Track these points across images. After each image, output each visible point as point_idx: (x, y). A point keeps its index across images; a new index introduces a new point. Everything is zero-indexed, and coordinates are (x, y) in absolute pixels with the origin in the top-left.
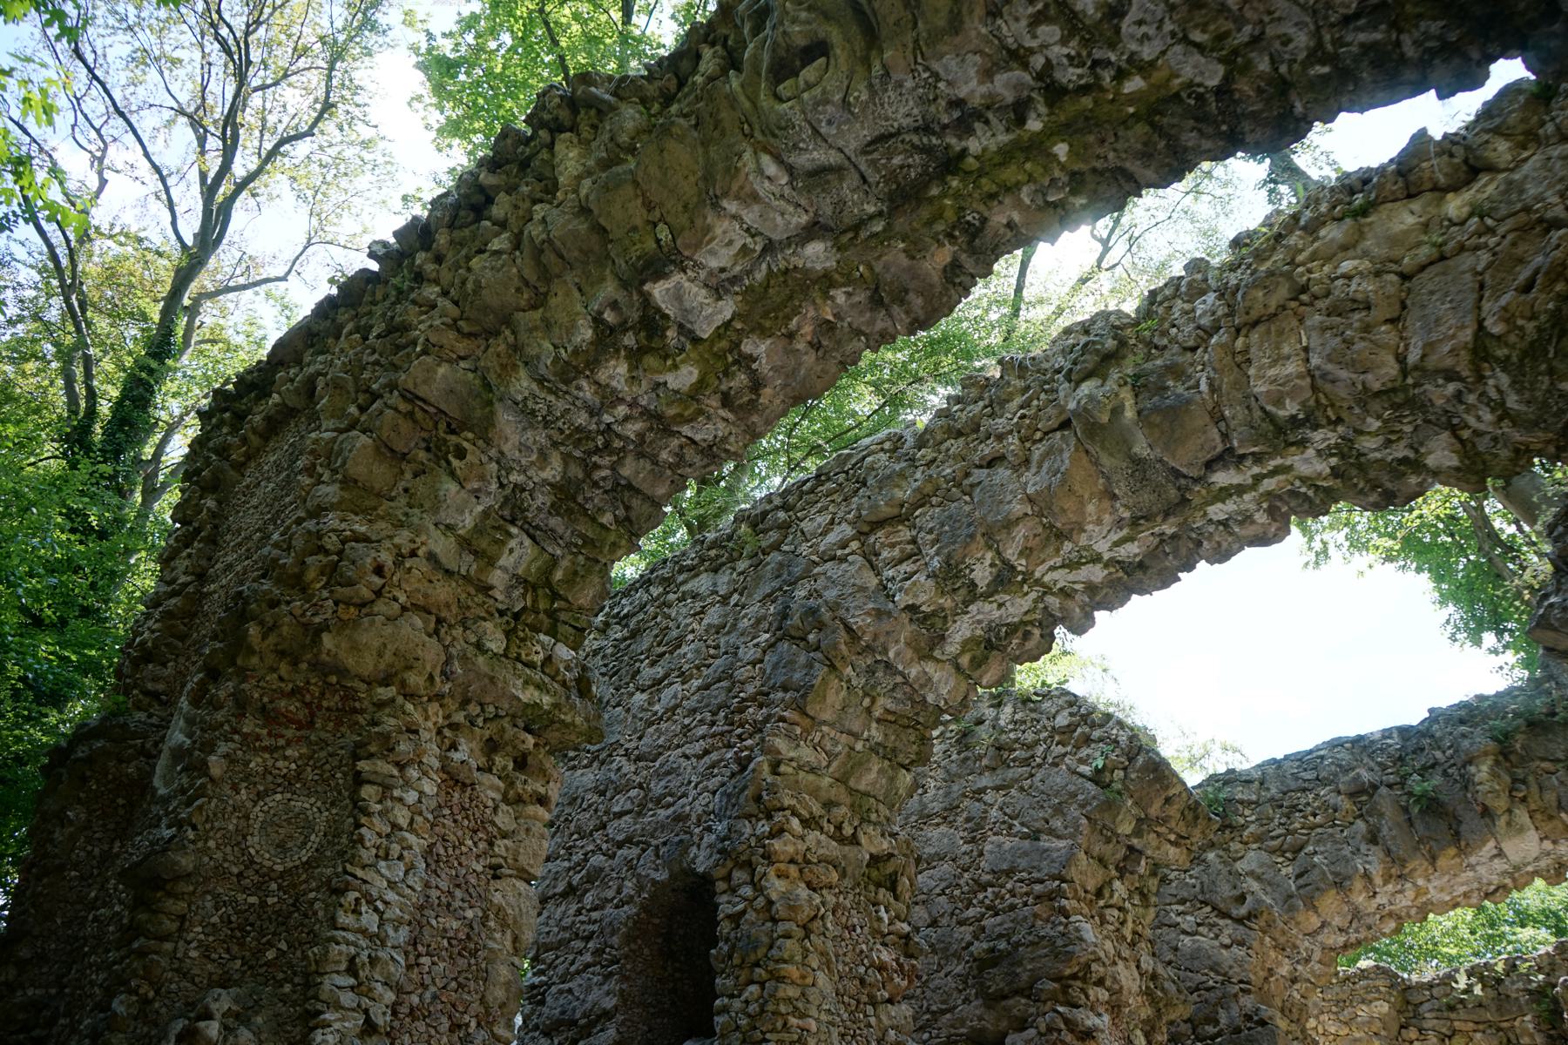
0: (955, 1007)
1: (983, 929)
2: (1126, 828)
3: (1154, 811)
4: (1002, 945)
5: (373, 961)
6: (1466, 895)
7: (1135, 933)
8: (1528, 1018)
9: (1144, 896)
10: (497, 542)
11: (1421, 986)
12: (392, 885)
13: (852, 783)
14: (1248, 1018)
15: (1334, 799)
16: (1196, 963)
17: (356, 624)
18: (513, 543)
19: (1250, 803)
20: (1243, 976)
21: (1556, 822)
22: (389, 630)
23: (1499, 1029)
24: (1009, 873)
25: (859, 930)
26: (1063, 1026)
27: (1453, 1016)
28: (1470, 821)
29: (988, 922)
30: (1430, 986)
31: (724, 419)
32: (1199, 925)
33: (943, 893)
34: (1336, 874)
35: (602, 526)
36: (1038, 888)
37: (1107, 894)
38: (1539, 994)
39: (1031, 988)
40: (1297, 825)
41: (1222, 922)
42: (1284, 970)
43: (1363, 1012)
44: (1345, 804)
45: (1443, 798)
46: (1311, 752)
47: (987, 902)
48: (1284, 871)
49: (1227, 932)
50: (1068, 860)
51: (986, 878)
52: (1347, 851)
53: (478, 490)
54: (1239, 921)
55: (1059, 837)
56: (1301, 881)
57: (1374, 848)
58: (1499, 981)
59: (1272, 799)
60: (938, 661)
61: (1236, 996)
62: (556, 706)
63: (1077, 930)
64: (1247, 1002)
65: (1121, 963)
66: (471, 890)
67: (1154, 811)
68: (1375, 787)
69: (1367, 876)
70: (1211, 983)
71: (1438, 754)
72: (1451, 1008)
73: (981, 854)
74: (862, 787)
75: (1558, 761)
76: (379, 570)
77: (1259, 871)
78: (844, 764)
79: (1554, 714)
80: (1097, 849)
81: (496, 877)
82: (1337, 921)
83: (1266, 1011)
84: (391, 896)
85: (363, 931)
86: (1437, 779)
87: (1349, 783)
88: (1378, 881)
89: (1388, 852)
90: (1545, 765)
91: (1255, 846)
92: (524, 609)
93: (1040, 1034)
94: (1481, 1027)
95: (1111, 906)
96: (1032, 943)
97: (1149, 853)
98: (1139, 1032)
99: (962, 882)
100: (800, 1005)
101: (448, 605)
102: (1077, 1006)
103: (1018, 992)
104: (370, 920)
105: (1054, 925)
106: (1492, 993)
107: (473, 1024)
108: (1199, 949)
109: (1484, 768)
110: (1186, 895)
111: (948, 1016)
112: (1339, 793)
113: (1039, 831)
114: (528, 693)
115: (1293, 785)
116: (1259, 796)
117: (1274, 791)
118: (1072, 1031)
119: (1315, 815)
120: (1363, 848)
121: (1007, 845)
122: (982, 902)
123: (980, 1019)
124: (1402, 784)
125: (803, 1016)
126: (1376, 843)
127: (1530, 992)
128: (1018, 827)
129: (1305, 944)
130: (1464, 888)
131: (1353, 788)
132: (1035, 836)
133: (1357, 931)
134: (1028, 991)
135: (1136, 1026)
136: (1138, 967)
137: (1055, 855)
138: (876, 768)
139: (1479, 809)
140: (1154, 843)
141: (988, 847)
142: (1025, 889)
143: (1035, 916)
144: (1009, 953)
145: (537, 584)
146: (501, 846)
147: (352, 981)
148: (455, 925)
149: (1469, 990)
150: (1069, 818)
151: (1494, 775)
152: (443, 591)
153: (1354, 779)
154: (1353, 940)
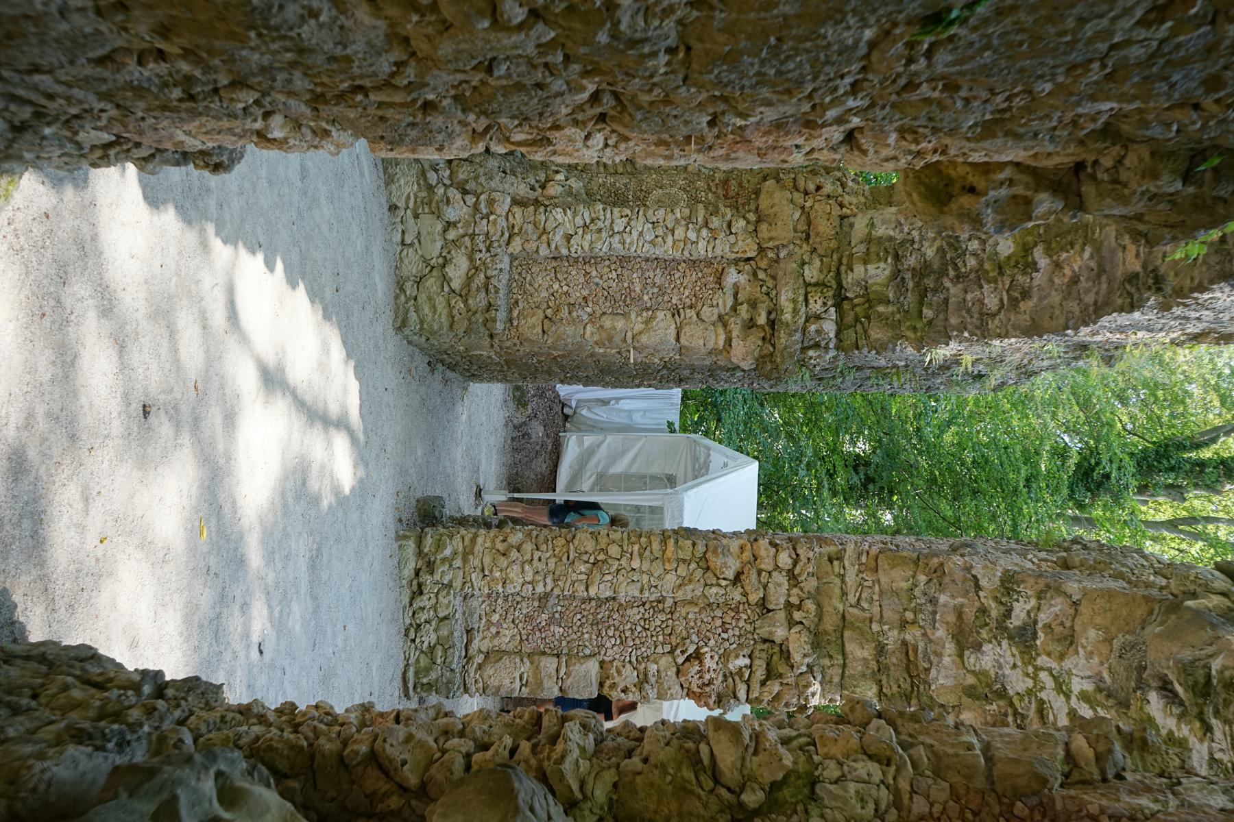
5: (600, 230)
10: (878, 255)
12: (641, 234)
13: (847, 634)
17: (784, 187)
18: (882, 265)
22: (784, 202)
25: (725, 636)
31: (1001, 300)
35: (920, 312)
53: (901, 225)
60: (961, 656)
62: (787, 325)
66: (660, 299)
74: (849, 647)
76: (818, 188)
78: (857, 619)
81: (673, 315)
84: (635, 234)
85: (612, 222)
92: (851, 299)
100: (647, 553)
101: (818, 234)
104: (619, 225)
107: (589, 310)
114: (787, 304)
125: (641, 556)
138: (866, 654)
145: (870, 299)
146: (691, 313)
147: (588, 222)
148: (638, 289)
152: (825, 227)
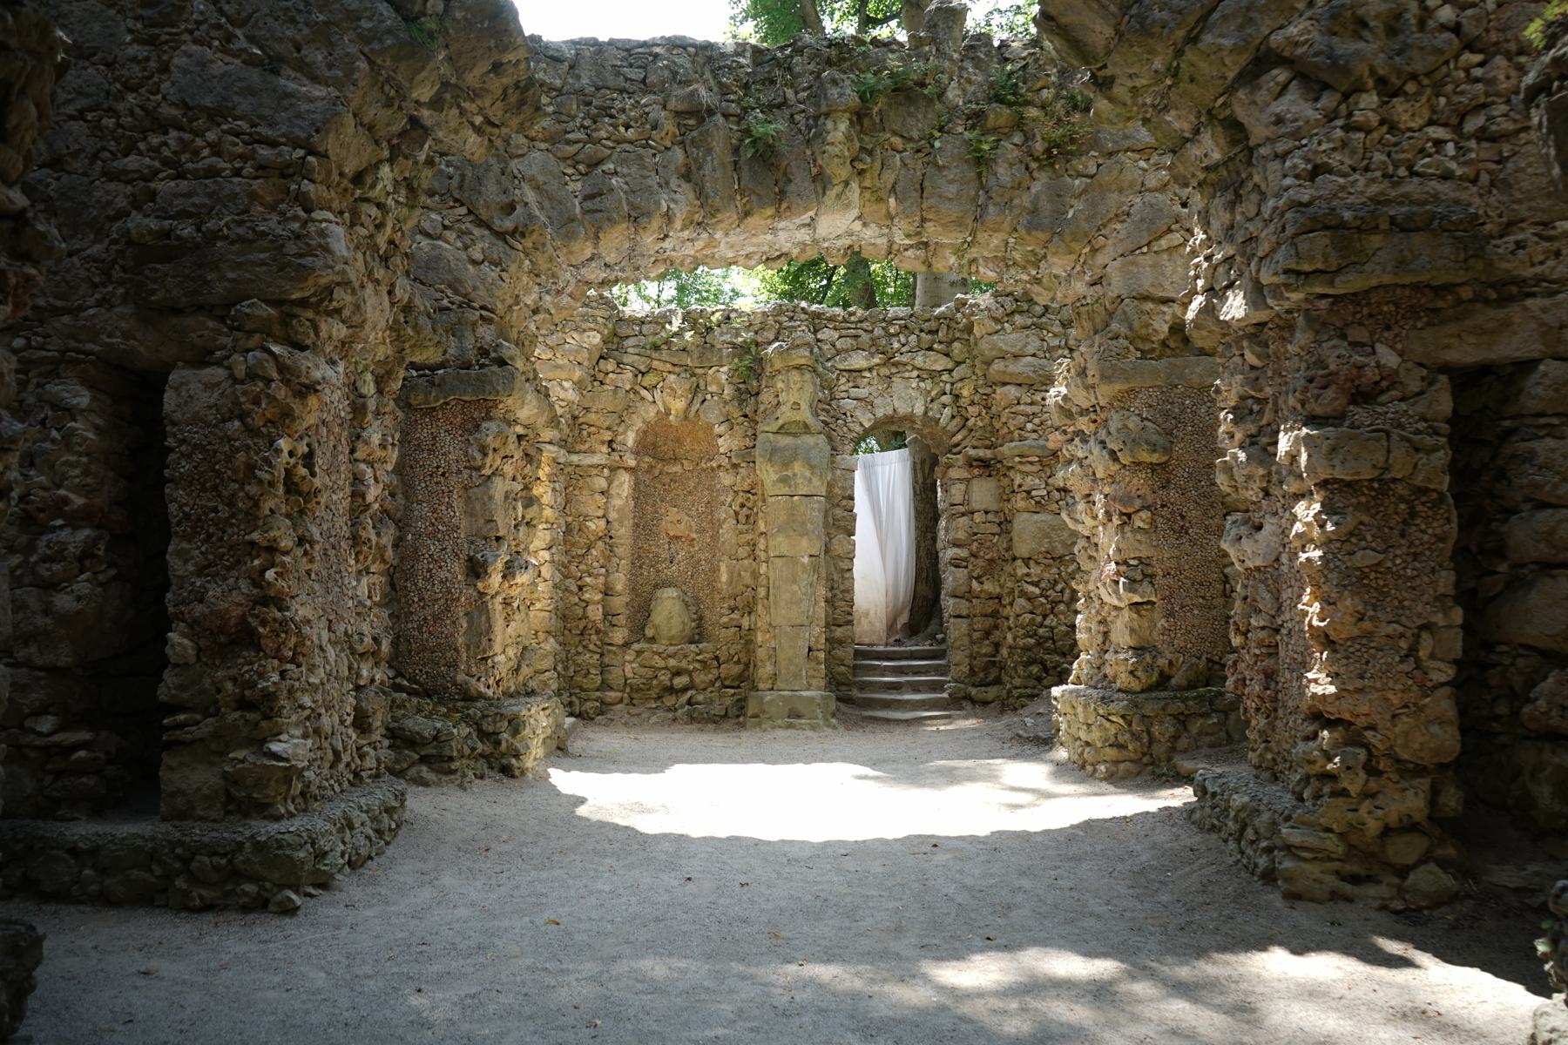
0: (81, 309)
1: (152, 195)
2: (425, 93)
3: (471, 79)
4: (187, 230)
6: (748, 256)
7: (391, 242)
8: (725, 369)
9: (412, 190)
11: (632, 321)
14: (484, 352)
15: (657, 113)
16: (431, 274)
19: (552, 88)
20: (488, 302)
21: (882, 208)
23: (693, 375)
24: (216, 115)
26: (275, 375)
27: (655, 355)
28: (801, 181)
29: (165, 186)
30: (642, 322)
32: (445, 227)
33: (80, 115)
34: (633, 207)
36: (264, 152)
37: (369, 181)
38: (743, 349)
39: (229, 306)
40: (603, 134)
41: (477, 232)
42: (530, 300)
43: (573, 339)
44: (669, 126)
45: (784, 148)
46: (644, 44)
47: (166, 153)
48: (572, 186)
49: (480, 245)
50: (326, 122)
51: (167, 111)
52: (653, 180)
54: (501, 235)
55: (315, 79)
56: (589, 205)
57: (685, 186)
58: (709, 329)
59: (580, 92)
61: (474, 324)
63: (323, 234)
64: (486, 333)
65: (370, 287)
67: (471, 79)
68: (711, 112)
69: (669, 217)
70: (445, 302)
71: (790, 93)
72: (656, 348)
73: (165, 69)
75: (911, 139)
77: (541, 179)
79: (923, 85)
80: (370, 114)
82: (610, 259)
83: (508, 350)
86: (779, 126)
87: (683, 99)
88: (678, 224)
89: (701, 194)
90: (897, 141)
91: (543, 146)
93: (232, 377)
94: (677, 370)
95: (367, 200)
96: (241, 239)
97: (440, 134)
98: (369, 377)
99: (120, 107)
102: (303, 348)
103: (200, 308)
105: (284, 219)
106: (700, 341)
108: (439, 258)
109: (843, 126)
110: (437, 185)
111: (66, 319)
112: (664, 107)
113: (281, 59)
115: (611, 80)
116: (565, 83)
117: (585, 81)
118: (287, 383)
119: (627, 127)
120: (674, 182)
121: (218, 68)
122: (156, 150)
123: (127, 335)
124: (740, 119)
126: (689, 181)
127: (734, 345)
128: (242, 43)
129: (567, 275)
130: (751, 249)
131: (680, 108)
132: (272, 64)
133: (622, 270)
134: (222, 311)
135: (366, 368)
136: (390, 293)
137: (304, 107)
139: (814, 171)
140: (453, 124)
141: (179, 61)
142: (240, 149)
143: (253, 196)
144: (197, 246)
149: (678, 334)
150: (339, 52)
151: (848, 138)
153: (693, 94)
154: (612, 278)
